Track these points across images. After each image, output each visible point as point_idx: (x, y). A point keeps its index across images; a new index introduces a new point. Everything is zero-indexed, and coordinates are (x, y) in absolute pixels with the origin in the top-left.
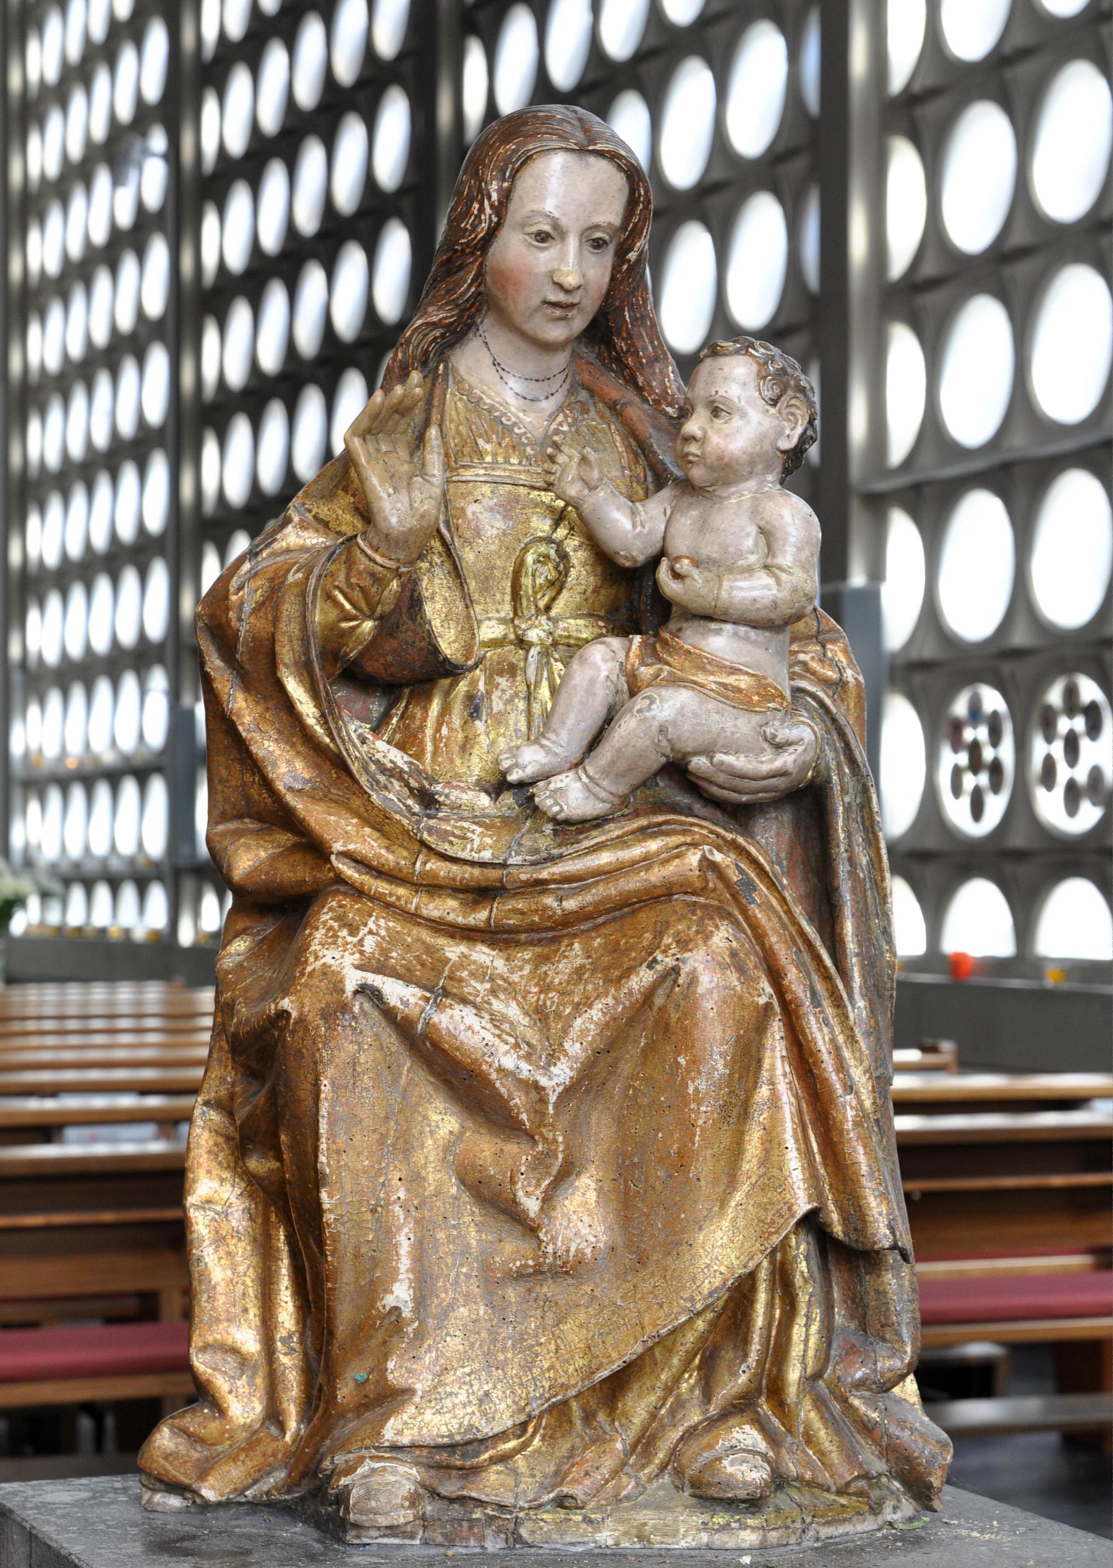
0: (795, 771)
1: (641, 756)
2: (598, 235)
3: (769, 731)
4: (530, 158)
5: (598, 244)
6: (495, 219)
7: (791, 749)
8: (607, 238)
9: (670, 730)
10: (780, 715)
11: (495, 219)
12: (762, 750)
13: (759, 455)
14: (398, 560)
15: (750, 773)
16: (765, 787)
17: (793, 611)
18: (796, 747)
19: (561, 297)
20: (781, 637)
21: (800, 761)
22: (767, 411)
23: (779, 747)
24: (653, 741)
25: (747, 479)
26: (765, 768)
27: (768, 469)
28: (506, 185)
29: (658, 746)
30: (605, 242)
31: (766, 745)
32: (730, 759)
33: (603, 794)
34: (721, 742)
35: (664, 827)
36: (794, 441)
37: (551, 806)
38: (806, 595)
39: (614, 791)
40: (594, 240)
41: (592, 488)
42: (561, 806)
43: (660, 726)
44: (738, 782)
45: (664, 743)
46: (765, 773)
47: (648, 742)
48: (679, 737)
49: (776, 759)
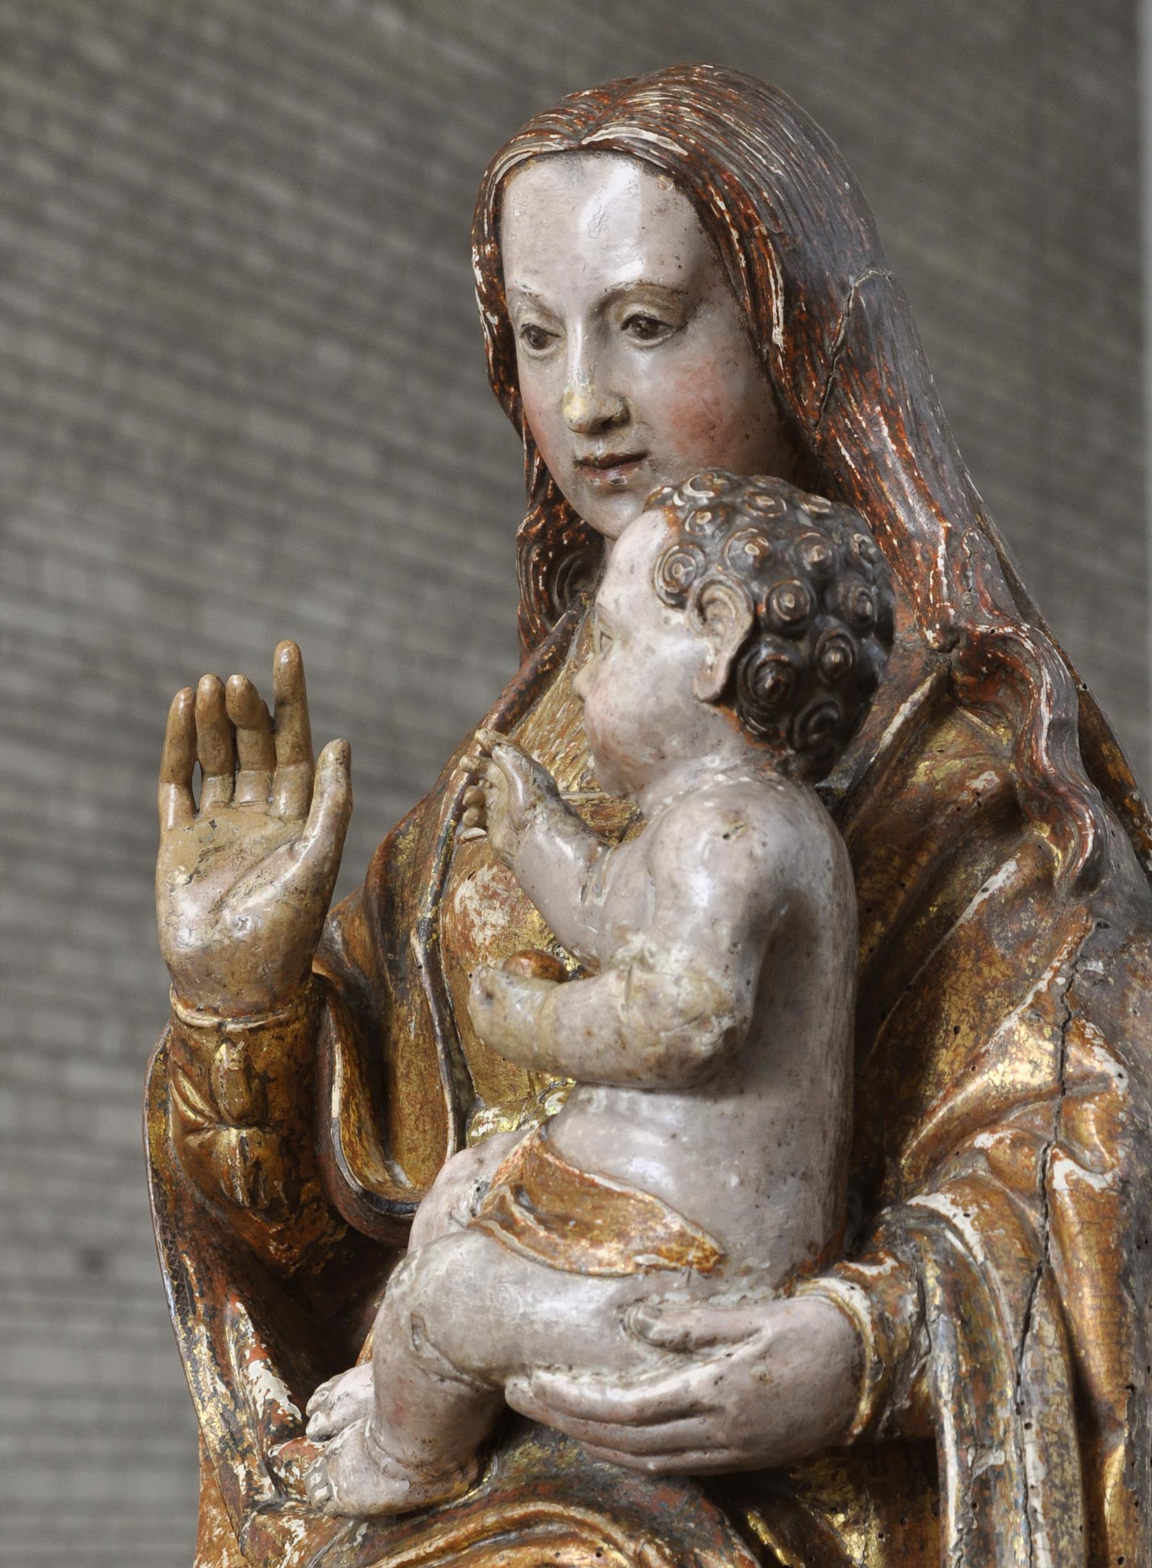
0: (730, 1402)
1: (401, 1381)
2: (635, 309)
3: (637, 1314)
4: (500, 189)
5: (646, 328)
6: (495, 320)
7: (721, 1351)
8: (653, 312)
9: (428, 1324)
10: (678, 1280)
11: (495, 320)
12: (628, 1361)
13: (657, 718)
14: (216, 1012)
15: (601, 1410)
16: (672, 1438)
17: (661, 1049)
18: (731, 1350)
19: (600, 449)
20: (728, 1106)
21: (746, 1380)
22: (667, 621)
23: (684, 1348)
24: (407, 1348)
25: (664, 772)
26: (628, 1398)
27: (697, 742)
28: (488, 248)
29: (419, 1358)
30: (653, 323)
31: (638, 1348)
32: (558, 1382)
33: (387, 1461)
34: (527, 1345)
35: (539, 1529)
36: (720, 677)
37: (316, 1487)
38: (681, 1012)
39: (400, 1455)
40: (633, 321)
41: (519, 827)
42: (330, 1490)
43: (412, 1315)
44: (594, 1427)
45: (428, 1352)
46: (632, 1411)
47: (400, 1352)
48: (446, 1336)
49: (666, 1376)
